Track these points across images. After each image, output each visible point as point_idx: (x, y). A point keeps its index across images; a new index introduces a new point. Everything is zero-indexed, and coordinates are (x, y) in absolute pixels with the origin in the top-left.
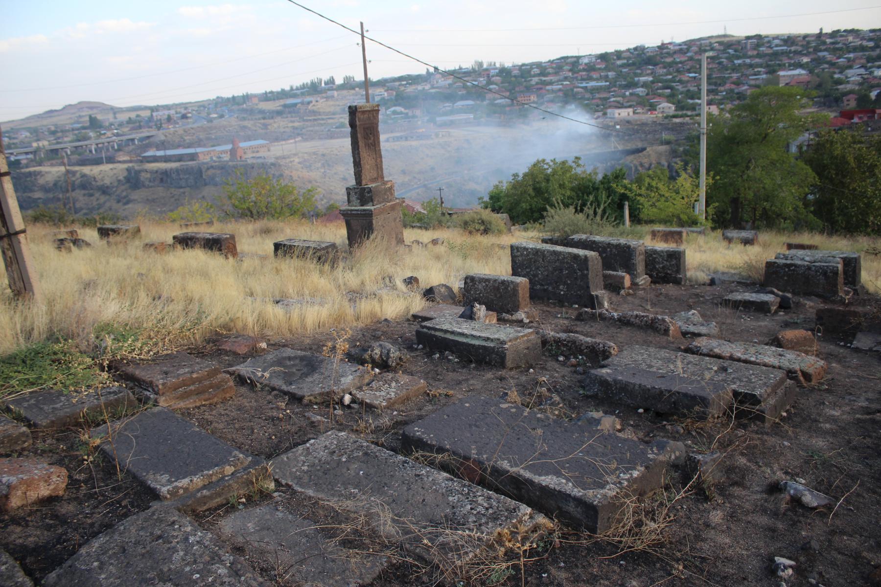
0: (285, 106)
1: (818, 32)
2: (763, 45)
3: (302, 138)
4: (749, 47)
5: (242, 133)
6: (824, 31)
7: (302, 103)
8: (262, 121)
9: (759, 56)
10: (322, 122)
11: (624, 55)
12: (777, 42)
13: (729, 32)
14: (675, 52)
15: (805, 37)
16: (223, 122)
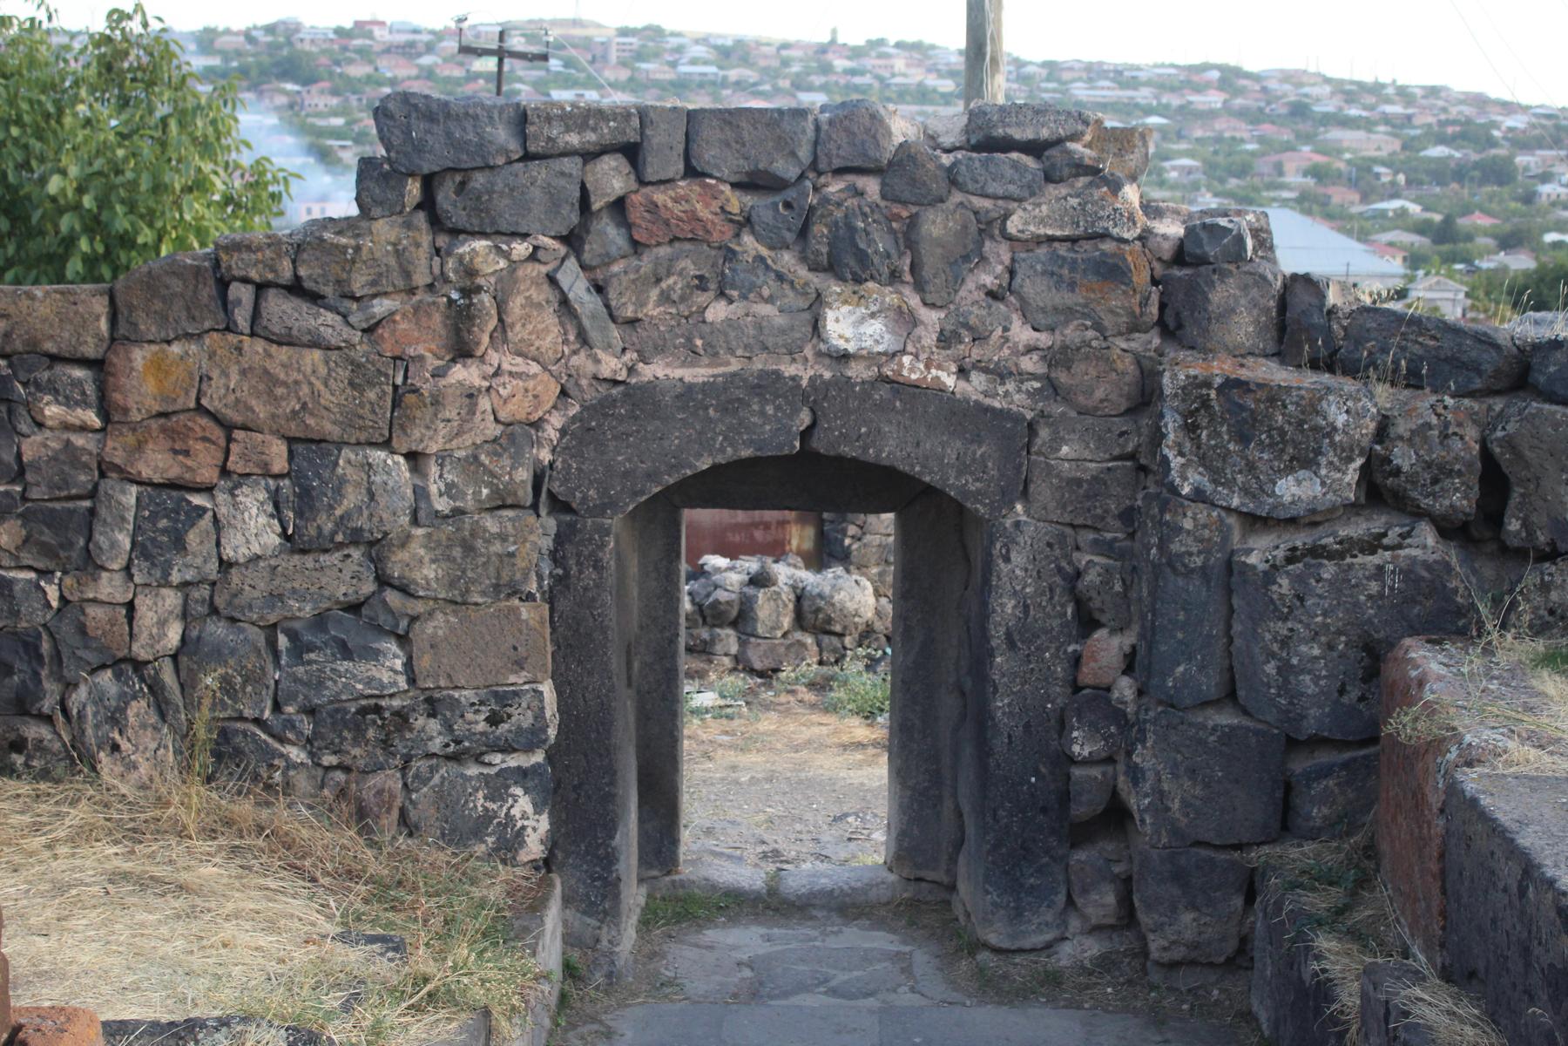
1: (826, 39)
2: (656, 55)
4: (613, 56)
6: (840, 40)
9: (632, 85)
11: (221, 42)
12: (699, 51)
13: (586, 16)
14: (389, 50)
15: (785, 46)
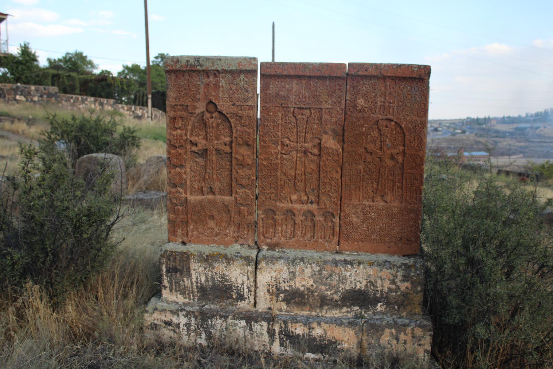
0: (517, 129)
3: (524, 155)
5: (475, 146)
7: (531, 128)
8: (495, 139)
10: (545, 144)
16: (463, 137)
